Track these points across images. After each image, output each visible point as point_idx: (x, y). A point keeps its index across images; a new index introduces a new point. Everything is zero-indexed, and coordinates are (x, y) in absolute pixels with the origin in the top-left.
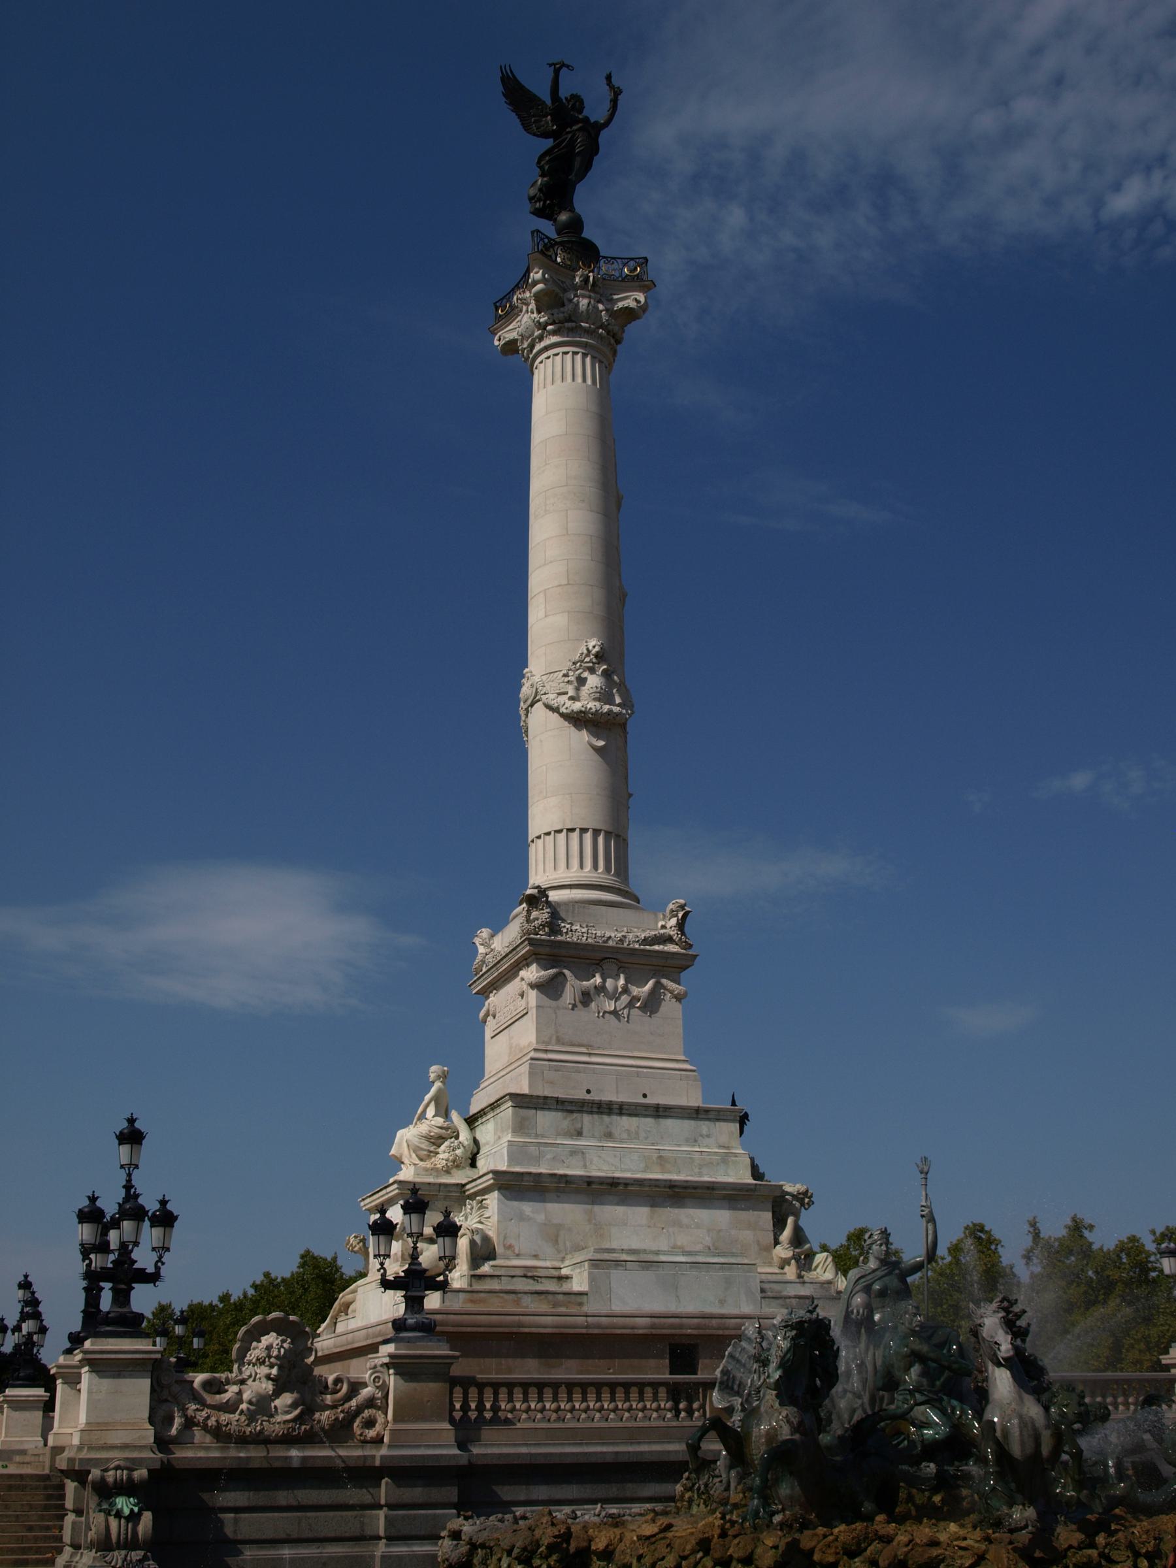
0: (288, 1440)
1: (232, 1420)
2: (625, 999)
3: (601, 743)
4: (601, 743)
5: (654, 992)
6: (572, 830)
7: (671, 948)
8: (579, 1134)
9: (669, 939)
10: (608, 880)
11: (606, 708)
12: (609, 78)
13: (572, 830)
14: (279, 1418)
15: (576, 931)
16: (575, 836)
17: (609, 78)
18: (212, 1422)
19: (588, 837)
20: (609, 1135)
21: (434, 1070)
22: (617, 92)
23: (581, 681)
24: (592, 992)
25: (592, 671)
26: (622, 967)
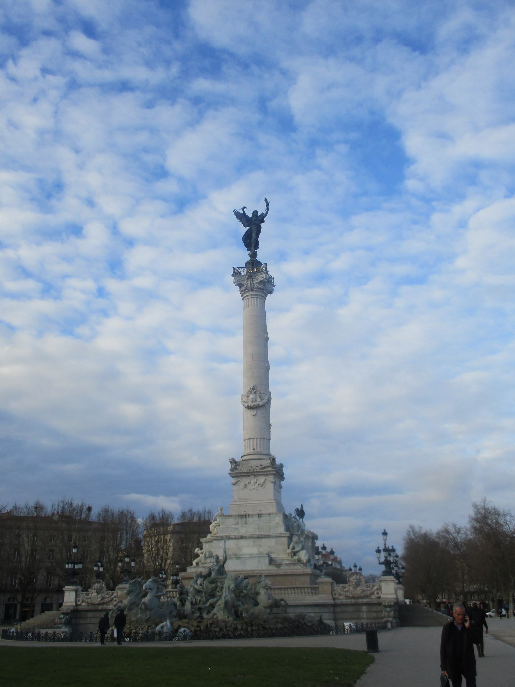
0: (99, 604)
1: (89, 600)
2: (256, 485)
3: (255, 413)
5: (264, 482)
7: (269, 469)
8: (238, 524)
9: (268, 467)
11: (253, 404)
12: (266, 200)
15: (243, 469)
16: (251, 440)
17: (266, 200)
20: (246, 523)
22: (267, 205)
23: (248, 396)
25: (250, 393)
26: (255, 476)
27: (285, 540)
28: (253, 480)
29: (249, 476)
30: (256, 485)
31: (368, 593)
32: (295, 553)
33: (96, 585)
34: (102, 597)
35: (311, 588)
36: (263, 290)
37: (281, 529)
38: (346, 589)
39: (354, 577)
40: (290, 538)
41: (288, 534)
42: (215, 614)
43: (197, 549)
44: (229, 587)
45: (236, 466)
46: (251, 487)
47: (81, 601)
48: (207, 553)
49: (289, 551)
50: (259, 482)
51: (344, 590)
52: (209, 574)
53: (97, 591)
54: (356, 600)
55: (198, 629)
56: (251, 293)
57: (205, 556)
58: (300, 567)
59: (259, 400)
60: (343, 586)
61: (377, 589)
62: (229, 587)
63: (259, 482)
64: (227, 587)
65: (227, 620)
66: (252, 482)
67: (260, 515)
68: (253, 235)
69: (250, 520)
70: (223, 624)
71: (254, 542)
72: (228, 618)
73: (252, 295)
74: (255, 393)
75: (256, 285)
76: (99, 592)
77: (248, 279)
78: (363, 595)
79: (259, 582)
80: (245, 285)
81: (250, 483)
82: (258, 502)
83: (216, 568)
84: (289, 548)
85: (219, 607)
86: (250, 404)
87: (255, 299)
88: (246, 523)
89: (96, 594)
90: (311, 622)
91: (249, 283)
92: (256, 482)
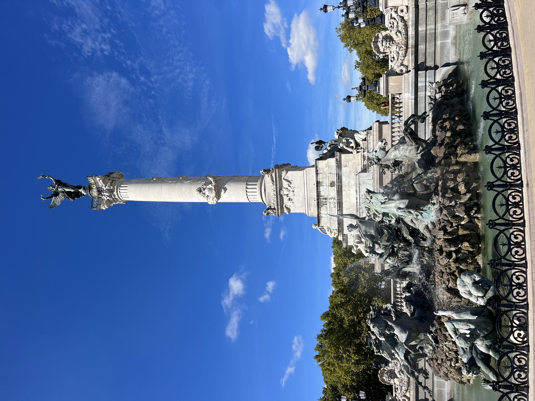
2: (289, 188)
4: (223, 190)
6: (246, 191)
7: (274, 175)
10: (258, 183)
13: (246, 191)
14: (403, 377)
18: (405, 392)
19: (248, 190)
21: (314, 227)
23: (208, 196)
24: (289, 198)
25: (204, 194)
26: (281, 189)
27: (343, 156)
28: (284, 192)
29: (281, 196)
30: (289, 188)
31: (401, 24)
32: (357, 145)
33: (384, 378)
34: (399, 372)
35: (392, 114)
36: (113, 181)
37: (332, 161)
38: (395, 56)
39: (380, 45)
40: (342, 151)
41: (338, 154)
42: (427, 227)
43: (353, 251)
44: (382, 203)
45: (271, 209)
46: (291, 195)
47: (404, 398)
48: (356, 241)
49: (355, 152)
50: (287, 186)
51: (396, 58)
52: (371, 237)
53: (391, 378)
54: (410, 46)
55: (454, 256)
56: (115, 193)
57: (358, 243)
58: (371, 137)
59: (210, 186)
60: (392, 61)
61: (396, 12)
62: (382, 203)
63: (287, 186)
64: (383, 206)
65: (437, 206)
66: (286, 193)
67: (318, 184)
68: (67, 190)
69: (322, 193)
70: (445, 212)
71: (344, 191)
72: (434, 204)
73: (117, 192)
74: (204, 189)
75: (107, 188)
76: (392, 375)
77: (102, 195)
78: (403, 32)
79: (379, 160)
80: (108, 198)
81: (287, 195)
82: (306, 187)
83: (363, 228)
84: (352, 153)
85: (415, 221)
86: (213, 194)
87: (121, 188)
88: (326, 199)
89: (396, 379)
90: (440, 88)
91: (105, 194)
92: (287, 188)
